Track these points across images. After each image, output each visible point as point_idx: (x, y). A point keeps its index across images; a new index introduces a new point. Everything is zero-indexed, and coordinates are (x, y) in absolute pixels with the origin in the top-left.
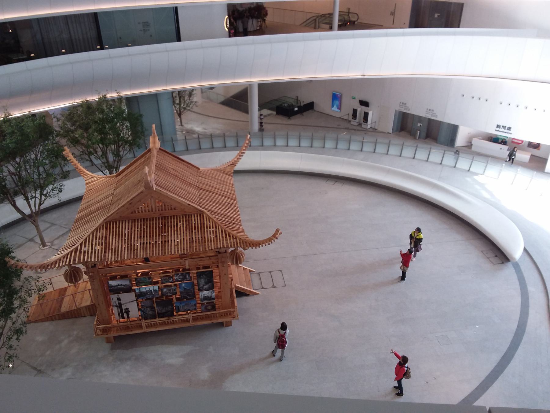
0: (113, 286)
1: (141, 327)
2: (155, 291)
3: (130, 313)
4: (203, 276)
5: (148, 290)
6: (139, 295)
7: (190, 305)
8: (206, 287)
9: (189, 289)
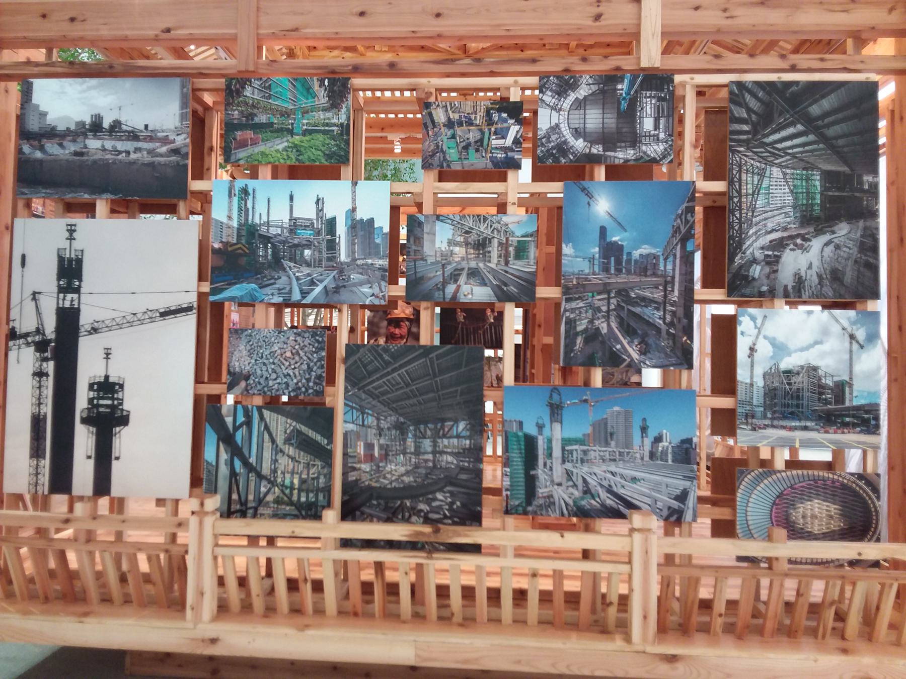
0: (51, 133)
1: (167, 590)
2: (362, 229)
3: (125, 441)
4: (789, 137)
5: (306, 211)
6: (235, 261)
7: (641, 446)
8: (806, 260)
9: (647, 266)
